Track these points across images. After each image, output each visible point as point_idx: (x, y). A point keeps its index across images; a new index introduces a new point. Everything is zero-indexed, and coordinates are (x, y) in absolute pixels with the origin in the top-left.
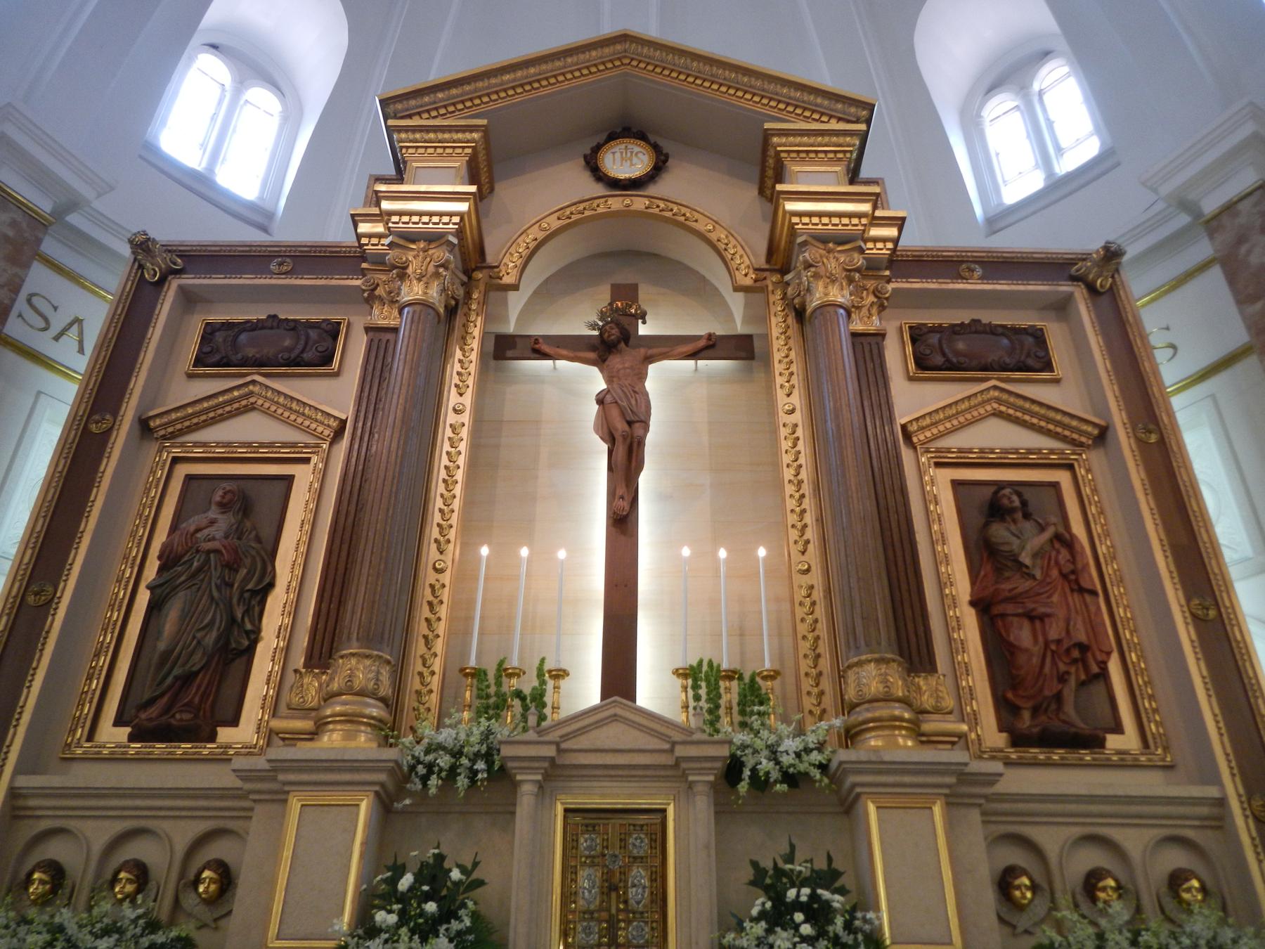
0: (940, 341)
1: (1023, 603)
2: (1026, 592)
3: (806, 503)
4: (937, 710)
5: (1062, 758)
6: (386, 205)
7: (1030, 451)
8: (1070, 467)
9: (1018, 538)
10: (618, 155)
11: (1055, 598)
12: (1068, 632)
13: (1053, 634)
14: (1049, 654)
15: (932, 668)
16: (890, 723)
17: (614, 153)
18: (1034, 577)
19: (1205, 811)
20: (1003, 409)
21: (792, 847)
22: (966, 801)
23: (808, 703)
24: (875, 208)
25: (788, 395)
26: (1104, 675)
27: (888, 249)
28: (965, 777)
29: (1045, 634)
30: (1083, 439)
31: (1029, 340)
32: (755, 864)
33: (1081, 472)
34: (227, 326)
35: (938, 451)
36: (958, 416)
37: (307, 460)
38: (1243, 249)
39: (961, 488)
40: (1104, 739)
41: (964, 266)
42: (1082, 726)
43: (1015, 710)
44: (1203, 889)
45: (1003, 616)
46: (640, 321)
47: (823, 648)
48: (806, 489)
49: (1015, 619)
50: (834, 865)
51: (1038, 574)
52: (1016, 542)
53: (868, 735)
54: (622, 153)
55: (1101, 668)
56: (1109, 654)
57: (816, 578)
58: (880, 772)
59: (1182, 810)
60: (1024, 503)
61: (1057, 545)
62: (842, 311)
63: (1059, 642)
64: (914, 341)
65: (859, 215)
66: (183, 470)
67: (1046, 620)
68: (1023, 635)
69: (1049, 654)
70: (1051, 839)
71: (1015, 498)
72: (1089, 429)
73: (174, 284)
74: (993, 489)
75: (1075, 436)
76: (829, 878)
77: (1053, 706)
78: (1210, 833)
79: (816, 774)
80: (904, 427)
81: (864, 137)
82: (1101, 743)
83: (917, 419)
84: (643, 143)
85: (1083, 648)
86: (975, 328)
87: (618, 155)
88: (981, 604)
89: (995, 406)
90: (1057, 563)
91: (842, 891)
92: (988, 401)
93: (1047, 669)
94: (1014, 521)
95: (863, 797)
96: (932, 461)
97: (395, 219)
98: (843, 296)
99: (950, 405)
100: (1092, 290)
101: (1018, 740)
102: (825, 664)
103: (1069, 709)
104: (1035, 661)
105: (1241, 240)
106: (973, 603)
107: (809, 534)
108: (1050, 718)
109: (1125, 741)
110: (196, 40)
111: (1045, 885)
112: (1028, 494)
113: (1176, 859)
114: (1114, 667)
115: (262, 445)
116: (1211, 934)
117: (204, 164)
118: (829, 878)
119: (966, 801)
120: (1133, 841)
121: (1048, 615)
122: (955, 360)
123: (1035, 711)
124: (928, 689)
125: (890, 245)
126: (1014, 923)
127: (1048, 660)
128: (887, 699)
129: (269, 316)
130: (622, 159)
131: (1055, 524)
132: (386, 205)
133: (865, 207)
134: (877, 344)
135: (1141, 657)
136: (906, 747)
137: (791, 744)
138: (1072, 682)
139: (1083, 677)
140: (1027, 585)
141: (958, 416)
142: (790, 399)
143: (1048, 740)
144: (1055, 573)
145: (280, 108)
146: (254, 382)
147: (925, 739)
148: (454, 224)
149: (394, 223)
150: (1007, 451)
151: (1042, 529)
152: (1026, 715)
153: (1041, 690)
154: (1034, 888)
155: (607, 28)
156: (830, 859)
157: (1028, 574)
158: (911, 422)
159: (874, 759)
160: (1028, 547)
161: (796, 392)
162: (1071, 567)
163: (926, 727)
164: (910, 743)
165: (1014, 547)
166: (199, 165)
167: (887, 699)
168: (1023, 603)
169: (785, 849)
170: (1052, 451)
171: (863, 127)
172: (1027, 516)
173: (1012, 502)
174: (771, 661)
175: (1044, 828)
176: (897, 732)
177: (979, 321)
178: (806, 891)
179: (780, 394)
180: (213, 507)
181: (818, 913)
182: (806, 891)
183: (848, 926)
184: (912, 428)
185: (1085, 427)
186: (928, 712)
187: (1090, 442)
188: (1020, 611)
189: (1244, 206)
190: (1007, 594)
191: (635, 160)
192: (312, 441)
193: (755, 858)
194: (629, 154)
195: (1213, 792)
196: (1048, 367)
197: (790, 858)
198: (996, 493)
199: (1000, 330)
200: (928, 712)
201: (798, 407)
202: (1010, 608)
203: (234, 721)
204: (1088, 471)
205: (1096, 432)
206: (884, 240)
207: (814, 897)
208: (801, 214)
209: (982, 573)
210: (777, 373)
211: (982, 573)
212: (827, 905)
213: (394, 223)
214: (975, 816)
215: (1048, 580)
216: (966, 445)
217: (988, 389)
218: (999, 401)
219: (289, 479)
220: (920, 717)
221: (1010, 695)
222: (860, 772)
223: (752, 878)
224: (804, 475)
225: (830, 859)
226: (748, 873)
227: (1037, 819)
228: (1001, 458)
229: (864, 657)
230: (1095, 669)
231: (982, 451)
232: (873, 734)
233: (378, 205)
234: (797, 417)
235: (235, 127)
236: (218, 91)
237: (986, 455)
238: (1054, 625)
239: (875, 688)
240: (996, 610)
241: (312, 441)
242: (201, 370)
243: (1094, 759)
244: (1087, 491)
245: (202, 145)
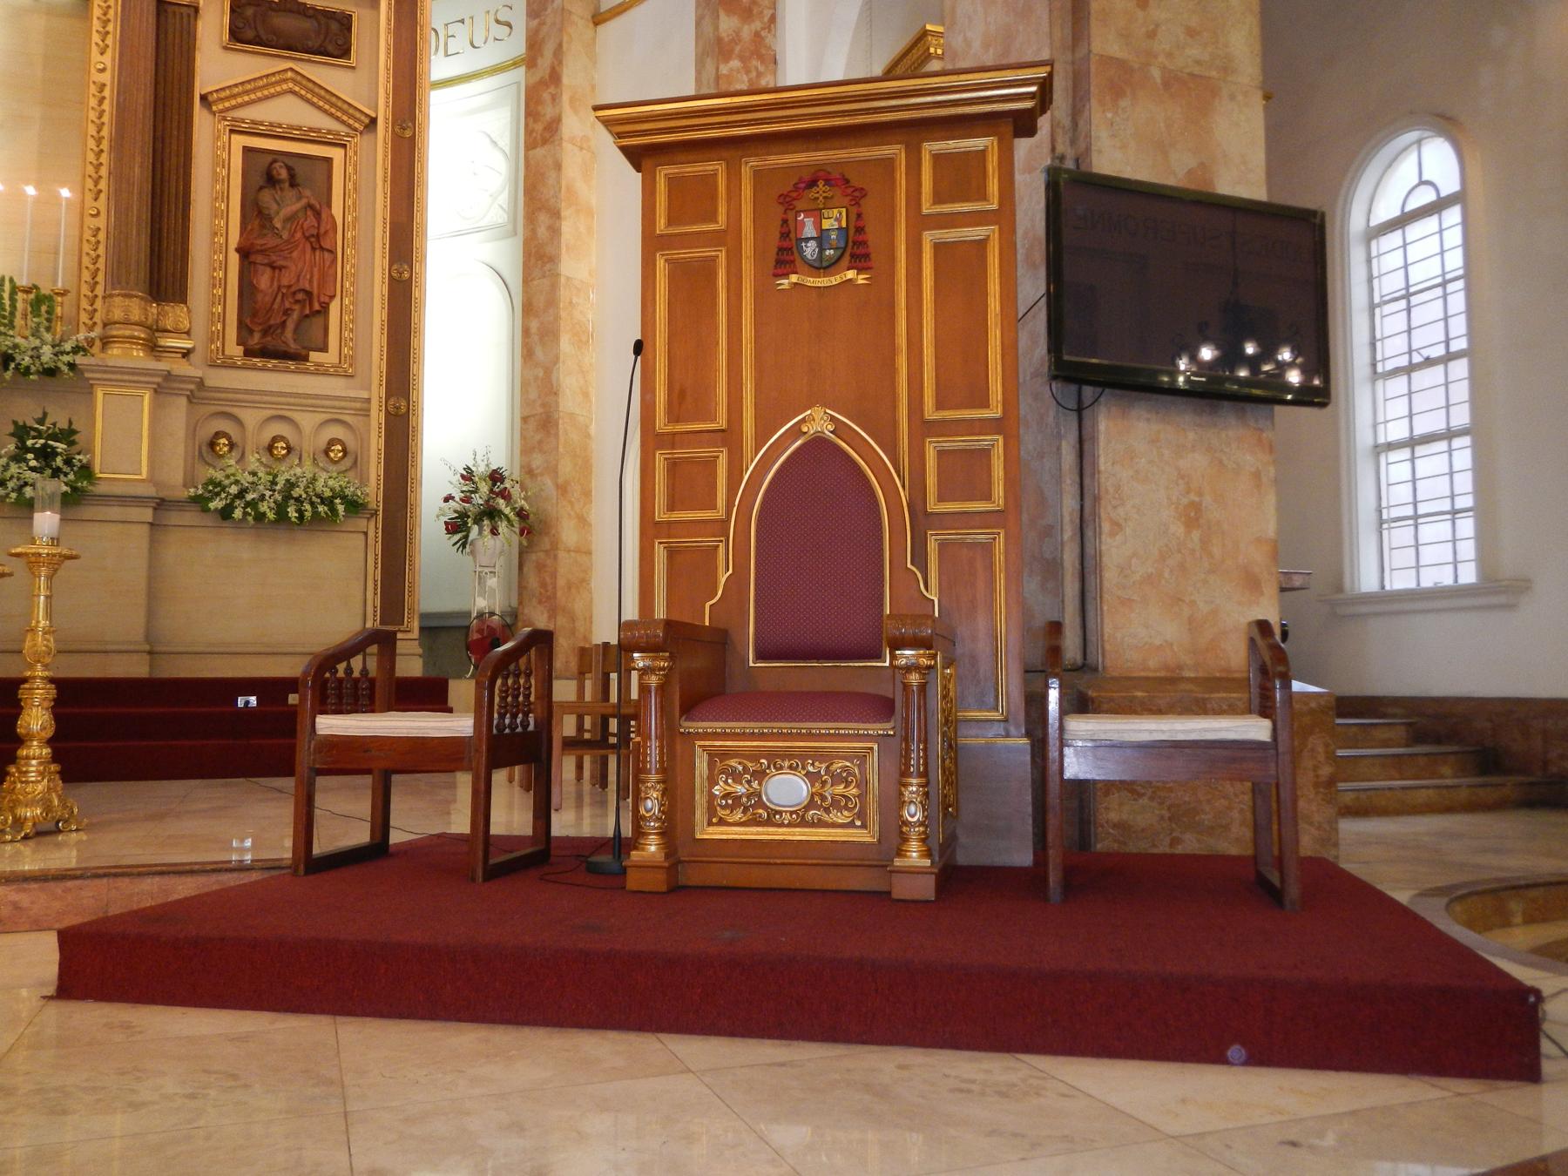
0: (255, 15)
1: (269, 255)
2: (273, 248)
3: (104, 158)
4: (177, 332)
5: (274, 366)
7: (311, 130)
8: (344, 146)
9: (279, 204)
11: (295, 254)
12: (298, 280)
13: (285, 282)
14: (280, 294)
16: (131, 339)
18: (281, 237)
19: (358, 405)
20: (297, 89)
21: (45, 415)
22: (176, 392)
23: (84, 317)
25: (102, 54)
26: (324, 310)
28: (168, 376)
29: (279, 280)
30: (357, 125)
31: (334, 26)
32: (15, 423)
33: (350, 153)
35: (234, 120)
36: (256, 89)
39: (250, 154)
40: (308, 356)
42: (293, 347)
43: (251, 332)
44: (345, 451)
45: (255, 263)
47: (100, 278)
48: (105, 145)
49: (262, 267)
50: (73, 427)
51: (285, 235)
52: (275, 206)
53: (112, 345)
55: (322, 307)
56: (332, 297)
57: (101, 222)
58: (105, 372)
59: (343, 404)
61: (309, 213)
63: (290, 287)
67: (283, 270)
68: (264, 280)
69: (280, 294)
70: (251, 417)
72: (363, 118)
74: (270, 158)
75: (351, 122)
76: (68, 435)
77: (279, 331)
78: (360, 418)
79: (65, 369)
80: (204, 98)
82: (306, 359)
83: (217, 91)
85: (309, 294)
88: (245, 252)
89: (291, 85)
90: (302, 228)
91: (71, 443)
92: (285, 81)
93: (276, 306)
94: (281, 189)
95: (95, 386)
96: (228, 128)
99: (249, 82)
101: (248, 353)
102: (99, 290)
103: (289, 333)
104: (268, 299)
106: (238, 250)
107: (103, 185)
108: (274, 339)
109: (329, 358)
111: (240, 444)
112: (301, 169)
113: (336, 432)
114: (334, 307)
116: (311, 475)
118: (68, 435)
119: (176, 392)
120: (307, 421)
121: (284, 267)
122: (264, 38)
123: (265, 333)
124: (174, 315)
126: (214, 464)
127: (279, 297)
128: (127, 323)
131: (307, 197)
134: (189, 16)
135: (352, 303)
136: (138, 356)
137: (47, 351)
138: (295, 316)
139: (307, 312)
140: (271, 241)
141: (256, 89)
142: (102, 59)
143: (265, 353)
144: (298, 235)
147: (153, 348)
150: (292, 127)
151: (299, 198)
152: (257, 337)
153: (269, 319)
154: (232, 446)
156: (70, 423)
157: (277, 234)
158: (211, 93)
159: (100, 363)
160: (282, 214)
161: (109, 52)
162: (315, 232)
163: (162, 342)
164: (141, 354)
165: (272, 212)
167: (127, 323)
168: (269, 255)
169: (40, 415)
170: (329, 132)
172: (293, 185)
173: (279, 174)
174: (63, 282)
175: (249, 410)
176: (134, 347)
178: (42, 441)
179: (94, 49)
181: (46, 454)
182: (42, 441)
183: (68, 462)
184: (210, 98)
185: (358, 115)
186: (170, 331)
187: (362, 128)
188: (266, 261)
190: (259, 248)
193: (15, 419)
195: (365, 395)
196: (345, 52)
197: (41, 421)
198: (271, 164)
199: (311, 12)
200: (170, 331)
201: (109, 66)
202: (259, 259)
204: (356, 153)
205: (367, 121)
207: (45, 446)
209: (250, 227)
210: (94, 29)
211: (250, 227)
212: (54, 448)
214: (183, 401)
215: (292, 240)
216: (258, 118)
217: (285, 71)
218: (293, 80)
220: (157, 334)
221: (248, 321)
222: (92, 371)
223: (12, 431)
224: (105, 132)
225: (70, 423)
226: (11, 429)
227: (243, 404)
228: (286, 133)
229: (117, 292)
230: (317, 307)
231: (271, 125)
232: (117, 345)
234: (106, 78)
237: (274, 129)
238: (287, 275)
239: (118, 314)
240: (253, 258)
243: (297, 368)
244: (350, 169)
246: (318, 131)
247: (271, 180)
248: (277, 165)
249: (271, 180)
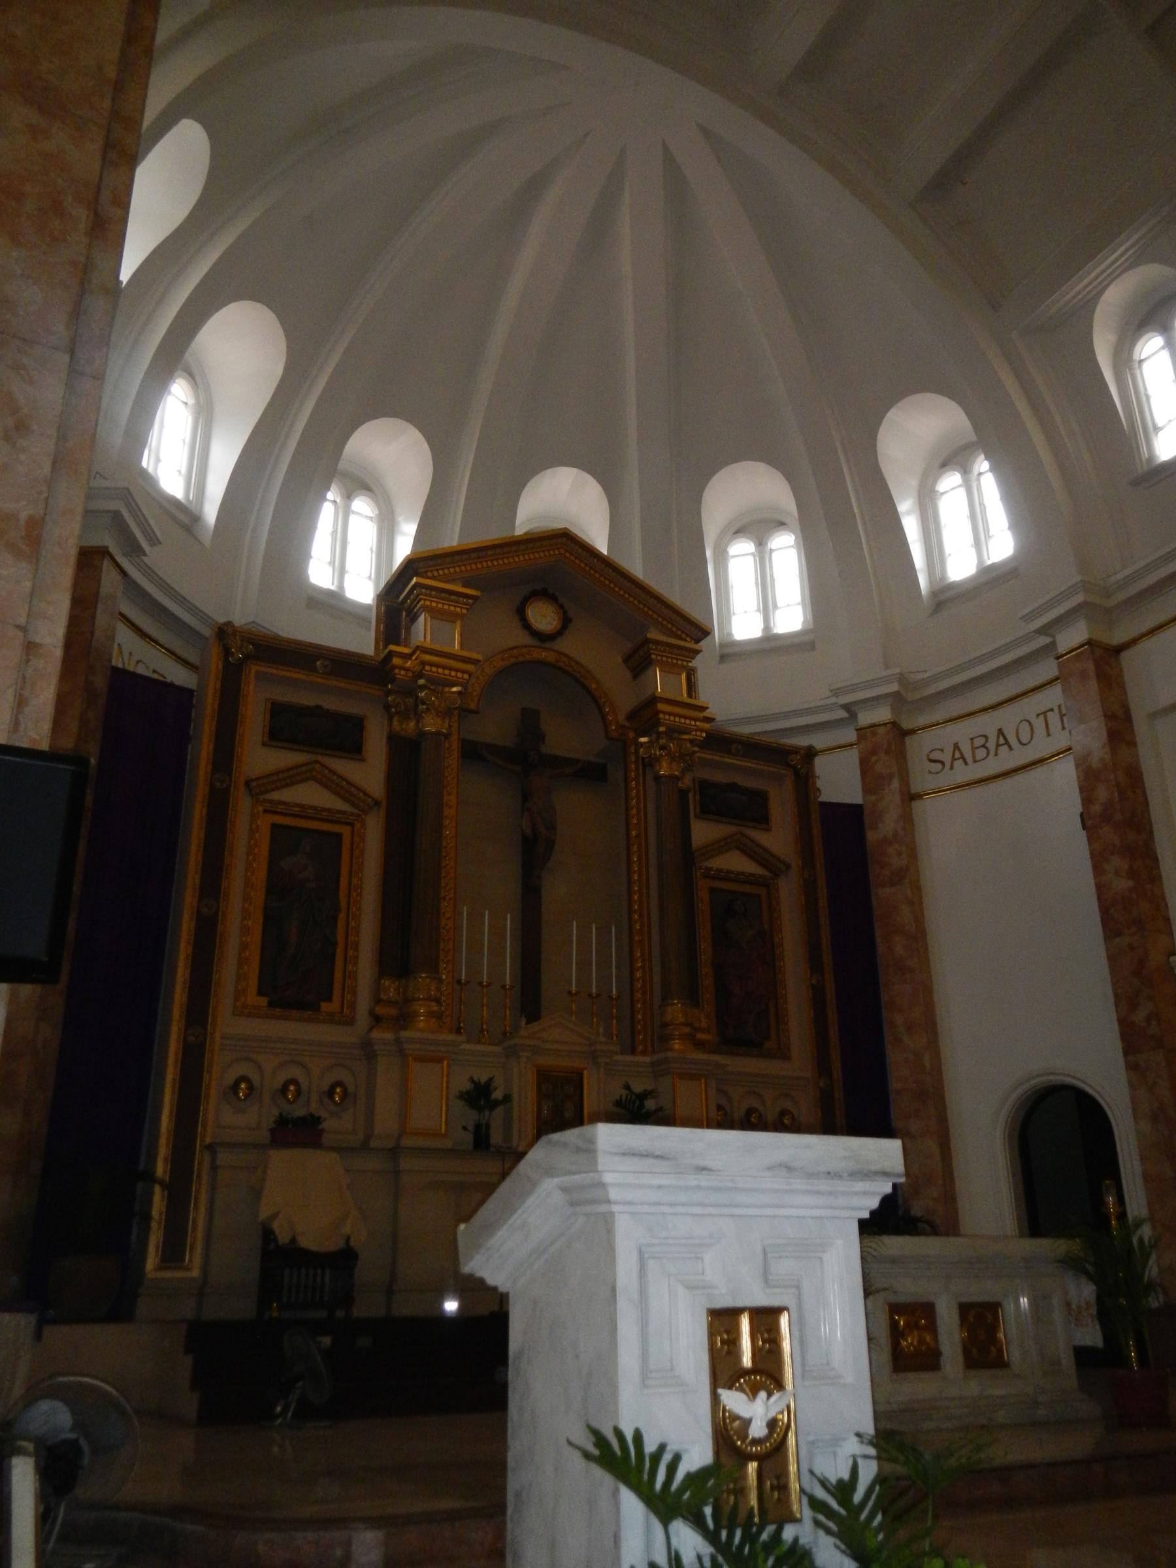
38: (874, 759)
73: (253, 669)
86: (733, 787)
97: (427, 668)
100: (797, 773)
105: (874, 752)
146: (317, 762)
189: (881, 730)
192: (356, 811)
203: (329, 999)
208: (665, 713)
241: (356, 811)
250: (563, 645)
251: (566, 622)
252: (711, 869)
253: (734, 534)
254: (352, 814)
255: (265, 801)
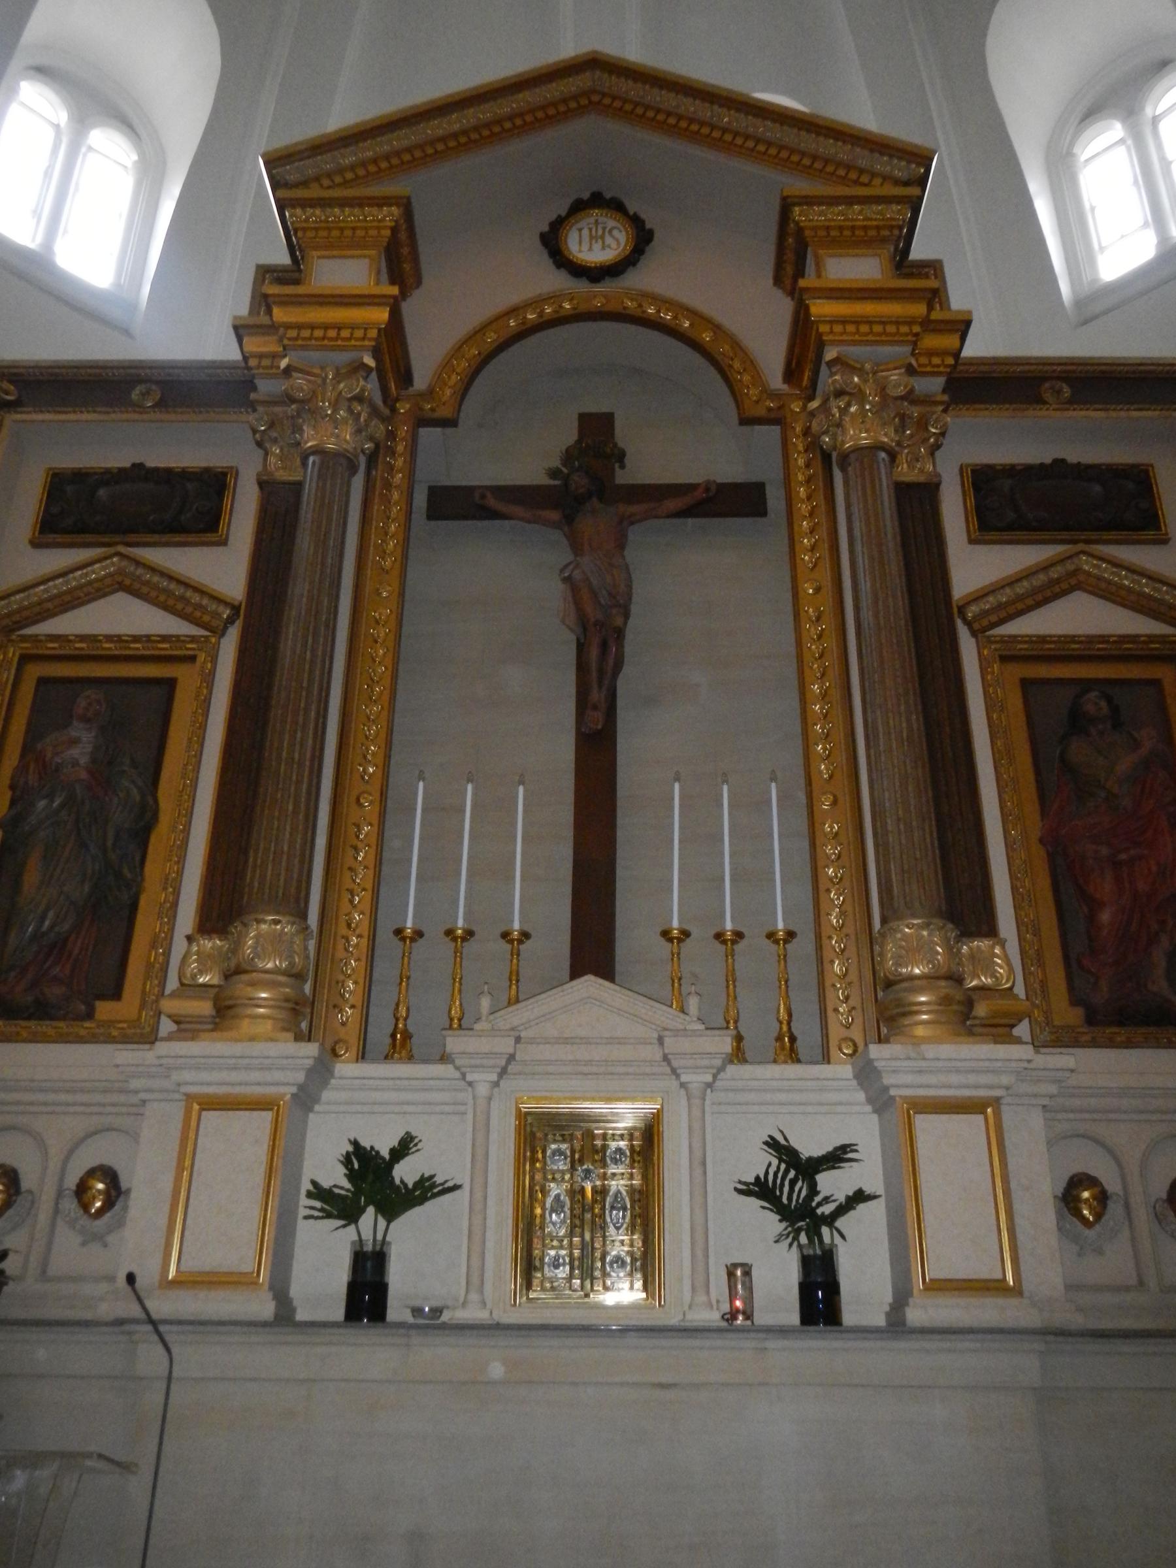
6: (279, 314)
10: (585, 232)
15: (990, 930)
17: (580, 230)
24: (930, 308)
27: (946, 366)
34: (79, 476)
37: (192, 659)
41: (1047, 385)
46: (617, 465)
54: (590, 230)
60: (1115, 710)
62: (883, 455)
64: (976, 487)
65: (910, 322)
66: (35, 671)
71: (1103, 704)
81: (915, 205)
84: (619, 215)
87: (585, 232)
97: (292, 333)
98: (886, 435)
101: (1091, 1019)
110: (18, 61)
115: (136, 639)
117: (39, 238)
125: (950, 361)
129: (134, 465)
130: (591, 237)
132: (279, 314)
133: (919, 309)
145: (135, 157)
148: (370, 339)
149: (290, 339)
155: (568, 49)
166: (33, 240)
170: (1152, 638)
171: (914, 191)
177: (1063, 461)
180: (75, 723)
191: (609, 240)
194: (600, 232)
203: (116, 994)
206: (943, 353)
213: (290, 339)
219: (170, 684)
233: (269, 312)
235: (77, 184)
236: (50, 134)
242: (51, 537)
245: (35, 212)
246: (1133, 639)
247: (1077, 722)
248: (1093, 695)
249: (1077, 722)
250: (641, 279)
251: (642, 239)
252: (1014, 638)
253: (1082, 121)
254: (193, 639)
255: (24, 638)
